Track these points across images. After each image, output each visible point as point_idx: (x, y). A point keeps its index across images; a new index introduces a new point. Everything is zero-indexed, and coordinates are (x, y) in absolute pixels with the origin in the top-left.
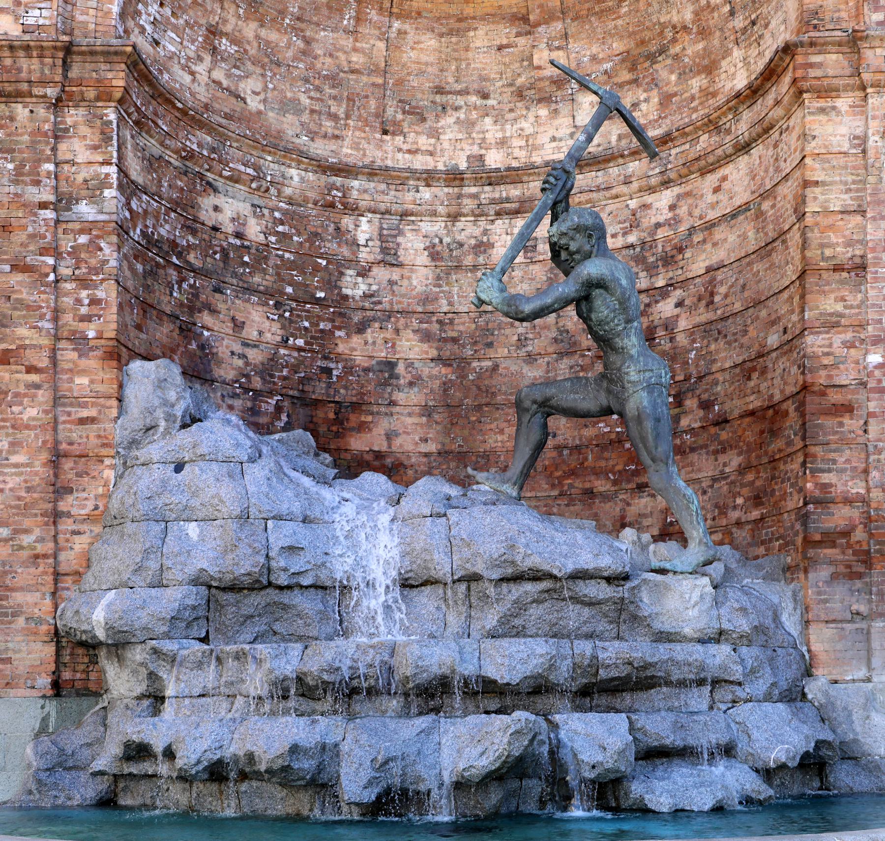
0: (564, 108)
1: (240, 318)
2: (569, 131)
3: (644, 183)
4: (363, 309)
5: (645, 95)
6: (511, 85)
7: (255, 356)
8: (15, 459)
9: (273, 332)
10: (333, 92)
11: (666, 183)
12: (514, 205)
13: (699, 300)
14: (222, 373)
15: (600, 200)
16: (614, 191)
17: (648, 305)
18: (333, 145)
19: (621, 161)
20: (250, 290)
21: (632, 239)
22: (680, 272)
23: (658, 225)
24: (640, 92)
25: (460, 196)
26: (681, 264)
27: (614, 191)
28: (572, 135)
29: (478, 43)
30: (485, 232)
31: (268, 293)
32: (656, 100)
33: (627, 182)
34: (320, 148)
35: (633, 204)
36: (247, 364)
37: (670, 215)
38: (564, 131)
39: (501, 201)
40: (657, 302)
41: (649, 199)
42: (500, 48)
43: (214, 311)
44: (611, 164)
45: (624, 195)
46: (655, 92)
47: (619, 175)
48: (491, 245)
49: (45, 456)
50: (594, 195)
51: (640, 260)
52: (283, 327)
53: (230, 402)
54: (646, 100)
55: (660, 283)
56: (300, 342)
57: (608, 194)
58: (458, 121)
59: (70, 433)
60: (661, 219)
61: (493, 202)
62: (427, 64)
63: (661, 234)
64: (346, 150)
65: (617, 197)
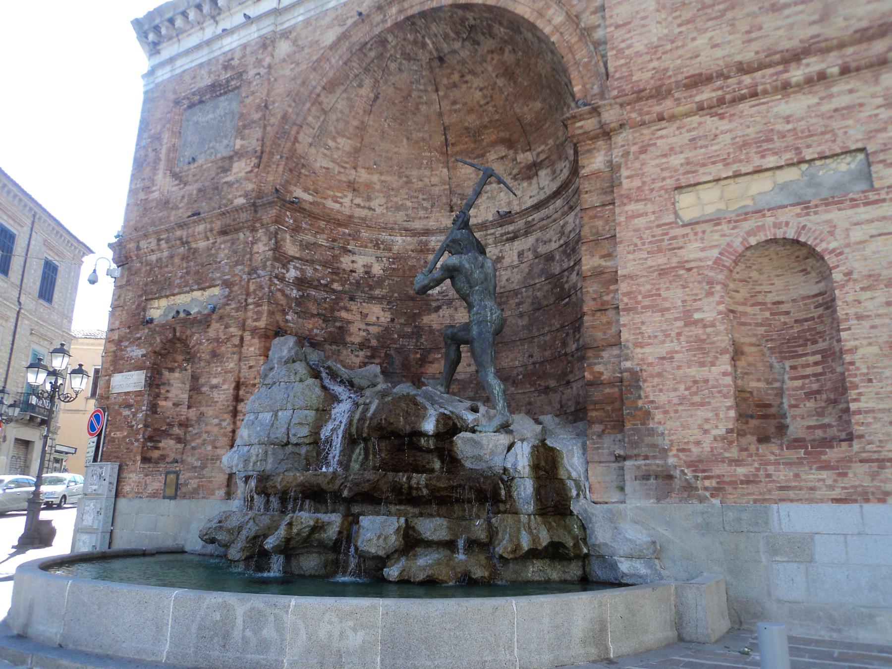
0: (534, 181)
1: (365, 311)
4: (438, 300)
6: (510, 174)
7: (373, 330)
8: (225, 387)
9: (385, 318)
10: (425, 197)
11: (571, 208)
12: (511, 235)
14: (352, 339)
16: (553, 217)
18: (425, 222)
20: (372, 298)
25: (486, 235)
27: (553, 217)
29: (492, 158)
30: (501, 251)
31: (383, 297)
34: (418, 225)
35: (562, 223)
36: (369, 334)
38: (535, 192)
39: (506, 234)
41: (567, 218)
42: (502, 158)
43: (347, 310)
48: (503, 257)
49: (233, 385)
50: (545, 222)
52: (392, 314)
53: (357, 353)
55: (572, 264)
56: (402, 321)
57: (550, 220)
58: (488, 198)
59: (245, 373)
61: (502, 235)
62: (470, 174)
64: (431, 224)
65: (555, 220)
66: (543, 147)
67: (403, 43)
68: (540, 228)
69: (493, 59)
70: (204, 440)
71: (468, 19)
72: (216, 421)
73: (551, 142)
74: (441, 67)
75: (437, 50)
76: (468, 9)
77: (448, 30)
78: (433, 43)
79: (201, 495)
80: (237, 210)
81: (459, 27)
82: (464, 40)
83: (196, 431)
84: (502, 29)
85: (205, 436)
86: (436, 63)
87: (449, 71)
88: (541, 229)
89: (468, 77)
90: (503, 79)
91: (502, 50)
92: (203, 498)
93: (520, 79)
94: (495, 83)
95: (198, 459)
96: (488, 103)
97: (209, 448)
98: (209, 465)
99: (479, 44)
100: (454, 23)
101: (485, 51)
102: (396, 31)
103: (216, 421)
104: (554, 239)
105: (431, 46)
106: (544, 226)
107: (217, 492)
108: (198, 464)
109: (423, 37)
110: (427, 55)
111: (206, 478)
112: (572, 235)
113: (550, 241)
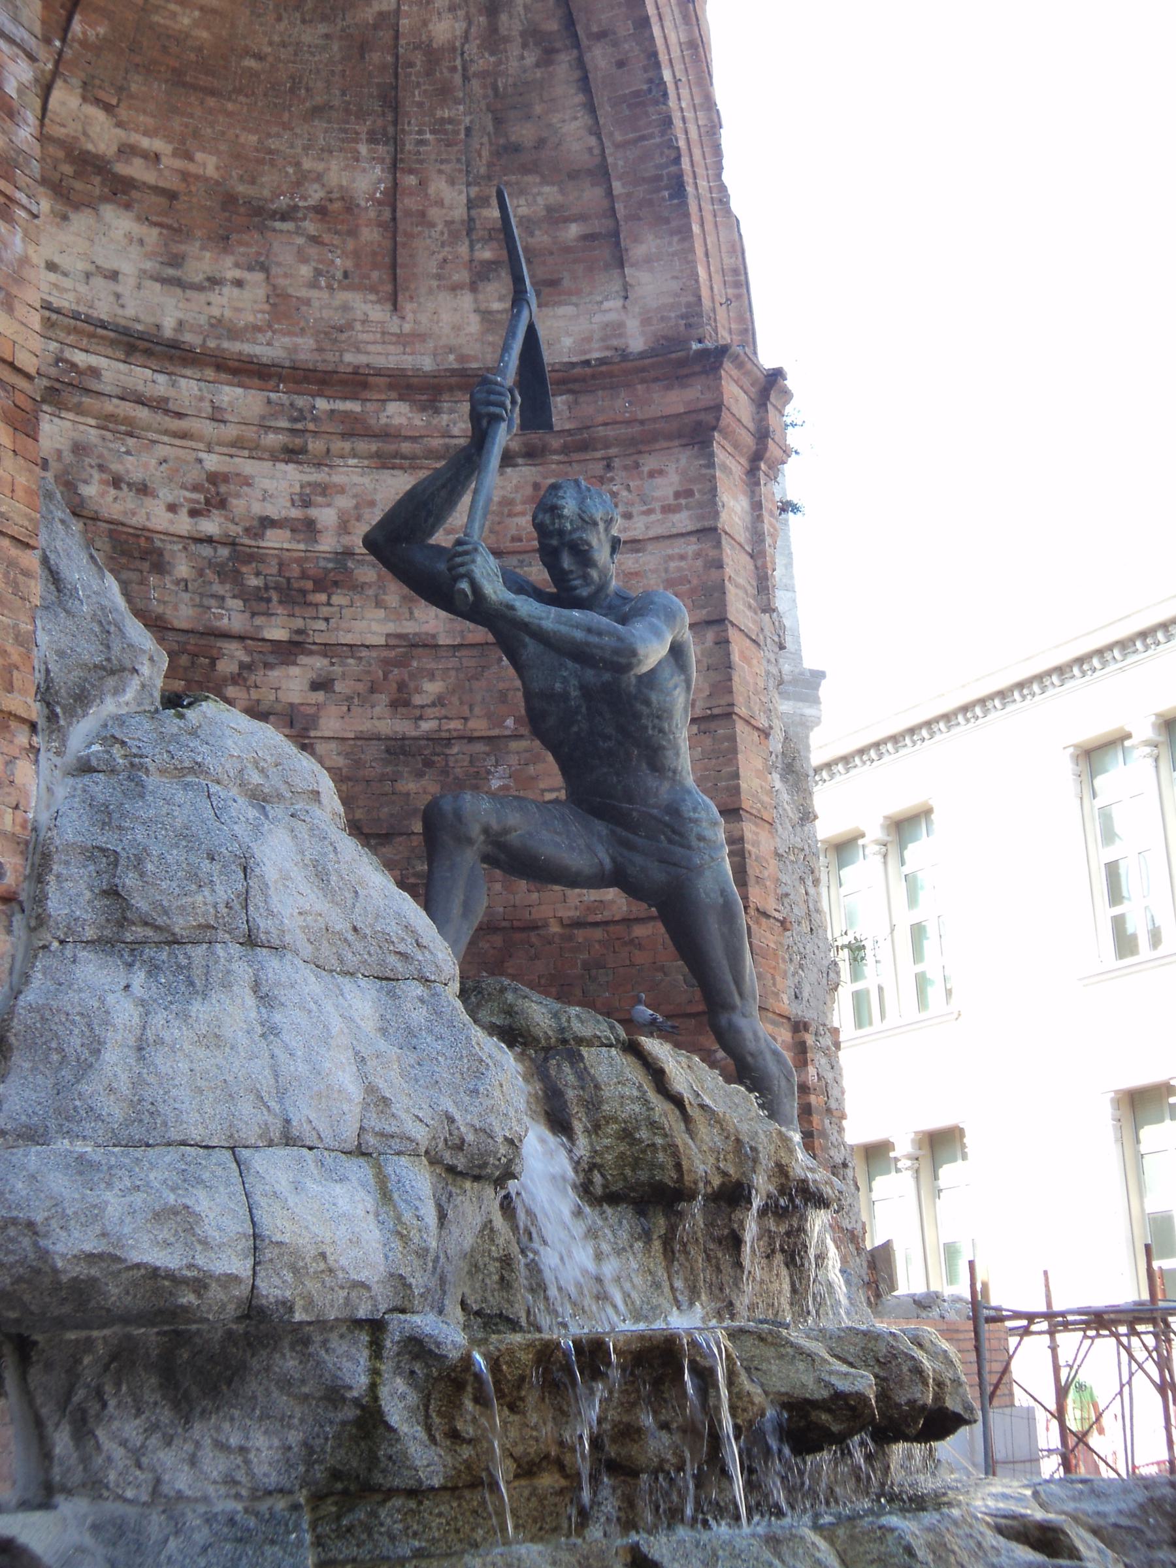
0: (81, 220)
2: (81, 266)
3: (250, 433)
5: (237, 274)
11: (291, 454)
13: (372, 690)
15: (148, 428)
16: (183, 424)
17: (242, 666)
19: (210, 373)
21: (210, 526)
22: (321, 625)
23: (267, 523)
24: (229, 261)
26: (325, 611)
27: (183, 424)
32: (261, 292)
35: (212, 462)
37: (295, 513)
40: (267, 666)
41: (249, 467)
44: (188, 372)
45: (200, 439)
46: (259, 276)
47: (201, 399)
51: (229, 573)
54: (239, 283)
55: (277, 632)
60: (272, 510)
63: (275, 540)
65: (184, 435)
66: (157, 145)
68: (111, 417)
73: (208, 164)
88: (107, 422)
104: (166, 494)
106: (128, 421)
112: (275, 540)
113: (143, 489)
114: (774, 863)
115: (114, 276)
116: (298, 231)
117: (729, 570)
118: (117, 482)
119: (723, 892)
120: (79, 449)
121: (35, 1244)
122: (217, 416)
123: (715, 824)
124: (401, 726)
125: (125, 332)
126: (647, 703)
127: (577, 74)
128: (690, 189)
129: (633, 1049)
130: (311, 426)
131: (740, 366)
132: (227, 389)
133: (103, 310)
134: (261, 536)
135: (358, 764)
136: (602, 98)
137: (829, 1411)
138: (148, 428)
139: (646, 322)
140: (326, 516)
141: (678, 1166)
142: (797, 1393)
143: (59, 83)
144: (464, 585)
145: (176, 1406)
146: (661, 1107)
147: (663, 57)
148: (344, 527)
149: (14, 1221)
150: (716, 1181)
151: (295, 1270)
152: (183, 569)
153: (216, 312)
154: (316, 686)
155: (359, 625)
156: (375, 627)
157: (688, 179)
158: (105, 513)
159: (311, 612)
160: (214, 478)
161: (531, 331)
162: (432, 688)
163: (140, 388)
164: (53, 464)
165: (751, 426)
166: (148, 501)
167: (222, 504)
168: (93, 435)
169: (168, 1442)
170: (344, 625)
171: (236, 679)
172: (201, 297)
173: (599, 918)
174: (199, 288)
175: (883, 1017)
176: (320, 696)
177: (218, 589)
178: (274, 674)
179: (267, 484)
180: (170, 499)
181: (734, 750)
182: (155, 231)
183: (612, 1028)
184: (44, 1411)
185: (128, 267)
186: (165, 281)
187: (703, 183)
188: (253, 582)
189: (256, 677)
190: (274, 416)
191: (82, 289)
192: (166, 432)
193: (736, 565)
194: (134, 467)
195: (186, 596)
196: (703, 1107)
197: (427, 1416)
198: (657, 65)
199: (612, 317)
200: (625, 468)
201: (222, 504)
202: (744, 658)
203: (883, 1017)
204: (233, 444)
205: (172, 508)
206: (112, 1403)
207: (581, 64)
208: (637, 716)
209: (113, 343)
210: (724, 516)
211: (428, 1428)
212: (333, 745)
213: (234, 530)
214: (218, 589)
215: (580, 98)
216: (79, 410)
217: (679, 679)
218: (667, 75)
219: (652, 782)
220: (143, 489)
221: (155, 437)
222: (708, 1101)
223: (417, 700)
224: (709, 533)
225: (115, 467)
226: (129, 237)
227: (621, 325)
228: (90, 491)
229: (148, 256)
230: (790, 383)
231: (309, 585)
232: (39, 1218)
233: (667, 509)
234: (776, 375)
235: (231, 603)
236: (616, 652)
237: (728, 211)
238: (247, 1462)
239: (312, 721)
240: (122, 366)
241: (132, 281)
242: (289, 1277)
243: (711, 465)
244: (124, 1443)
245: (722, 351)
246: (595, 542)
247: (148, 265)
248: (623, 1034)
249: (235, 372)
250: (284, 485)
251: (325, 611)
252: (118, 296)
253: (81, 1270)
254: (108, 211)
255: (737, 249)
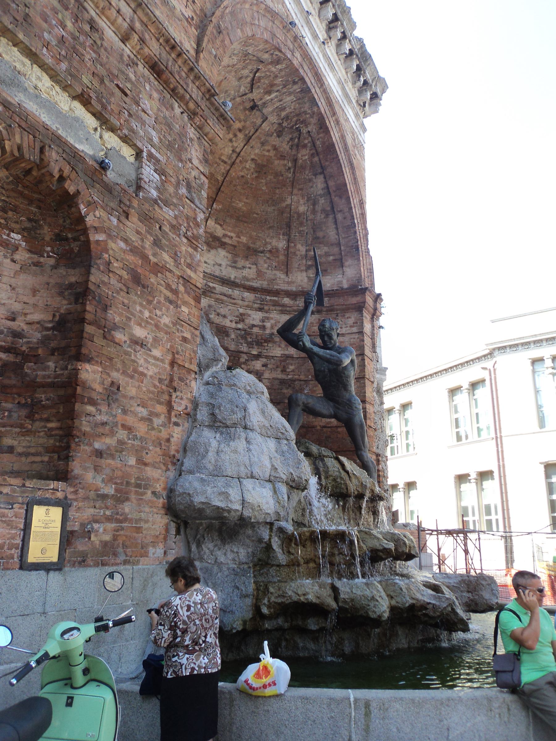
0: (213, 252)
2: (213, 263)
3: (251, 304)
5: (250, 266)
11: (260, 309)
13: (277, 367)
15: (226, 302)
16: (235, 301)
17: (246, 360)
19: (242, 289)
21: (240, 326)
22: (265, 351)
23: (254, 326)
24: (248, 262)
27: (235, 301)
28: (214, 265)
32: (255, 270)
33: (243, 300)
35: (241, 311)
37: (260, 324)
40: (252, 360)
41: (250, 312)
46: (255, 266)
47: (239, 295)
51: (244, 337)
54: (250, 268)
55: (255, 352)
65: (235, 304)
66: (232, 234)
67: (272, 75)
68: (217, 299)
69: (268, 151)
70: (121, 442)
71: (306, 126)
72: (143, 412)
73: (244, 239)
74: (245, 109)
75: (264, 103)
76: (321, 128)
77: (288, 110)
78: (272, 100)
79: (122, 558)
80: (191, 69)
81: (295, 119)
82: (280, 124)
83: (104, 418)
84: (307, 157)
85: (122, 434)
86: (248, 105)
87: (242, 118)
88: (217, 300)
89: (240, 136)
90: (253, 166)
91: (282, 157)
92: (125, 562)
93: (263, 181)
94: (247, 161)
95: (110, 480)
96: (225, 163)
97: (132, 461)
98: (133, 496)
99: (279, 136)
100: (297, 115)
101: (274, 143)
102: (288, 70)
103: (143, 412)
105: (269, 98)
106: (221, 300)
107: (151, 550)
108: (110, 490)
109: (277, 91)
110: (258, 97)
111: (131, 520)
112: (255, 330)
113: (224, 316)
114: (373, 414)
115: (220, 265)
116: (265, 256)
117: (365, 342)
118: (218, 314)
119: (361, 421)
120: (210, 306)
121: (190, 499)
122: (243, 300)
123: (360, 404)
124: (284, 377)
125: (222, 279)
126: (344, 374)
127: (334, 220)
128: (360, 249)
129: (337, 459)
130: (265, 303)
131: (370, 292)
132: (246, 293)
133: (217, 273)
134: (252, 329)
135: (273, 385)
136: (340, 226)
137: (382, 552)
138: (226, 302)
139: (348, 281)
140: (268, 325)
141: (347, 489)
142: (375, 547)
143: (210, 219)
144: (301, 343)
145: (222, 540)
146: (343, 473)
147: (355, 217)
148: (272, 327)
149: (185, 493)
150: (356, 493)
151: (252, 509)
152: (233, 336)
153: (244, 274)
154: (263, 366)
155: (274, 351)
156: (278, 352)
157: (360, 246)
158: (215, 322)
159: (263, 348)
160: (242, 314)
161: (320, 282)
162: (292, 368)
163: (225, 292)
164: (203, 310)
165: (372, 307)
166: (226, 319)
167: (243, 321)
168: (213, 303)
169: (219, 549)
170: (271, 351)
171: (244, 363)
172: (241, 271)
173: (329, 426)
174: (240, 269)
175: (547, 538)
176: (264, 368)
177: (241, 341)
178: (254, 362)
179: (254, 316)
180: (231, 319)
181: (365, 386)
182: (231, 255)
183: (332, 454)
184: (190, 540)
185: (224, 264)
186: (232, 267)
187: (363, 248)
188: (249, 340)
189: (249, 363)
190: (257, 300)
191: (213, 268)
192: (231, 303)
193: (367, 341)
194: (222, 311)
195: (233, 343)
196: (354, 474)
197: (283, 547)
198: (354, 219)
199: (339, 279)
200: (341, 316)
201: (243, 321)
202: (368, 363)
203: (547, 538)
204: (247, 306)
205: (231, 321)
206: (206, 539)
207: (335, 218)
208: (342, 377)
209: (219, 281)
210: (365, 329)
211: (283, 550)
212: (267, 380)
213: (246, 327)
214: (241, 341)
215: (334, 226)
216: (210, 297)
217: (352, 368)
218: (356, 221)
219: (345, 393)
220: (224, 316)
221: (228, 304)
222: (355, 473)
223: (288, 370)
224: (361, 333)
225: (218, 311)
226: (224, 256)
227: (342, 281)
228: (212, 316)
229: (229, 261)
230: (383, 297)
231: (263, 341)
232: (191, 493)
233: (351, 327)
234: (379, 295)
235: (244, 345)
236: (337, 361)
237: (369, 255)
238: (238, 555)
239: (262, 374)
240: (221, 287)
241: (224, 267)
242: (251, 511)
243: (362, 316)
244: (209, 549)
245: (366, 289)
246: (333, 334)
247: (229, 263)
248: (335, 455)
249: (248, 289)
250: (258, 317)
251: (266, 348)
252: (221, 270)
253: (201, 506)
254: (220, 250)
255: (371, 264)
